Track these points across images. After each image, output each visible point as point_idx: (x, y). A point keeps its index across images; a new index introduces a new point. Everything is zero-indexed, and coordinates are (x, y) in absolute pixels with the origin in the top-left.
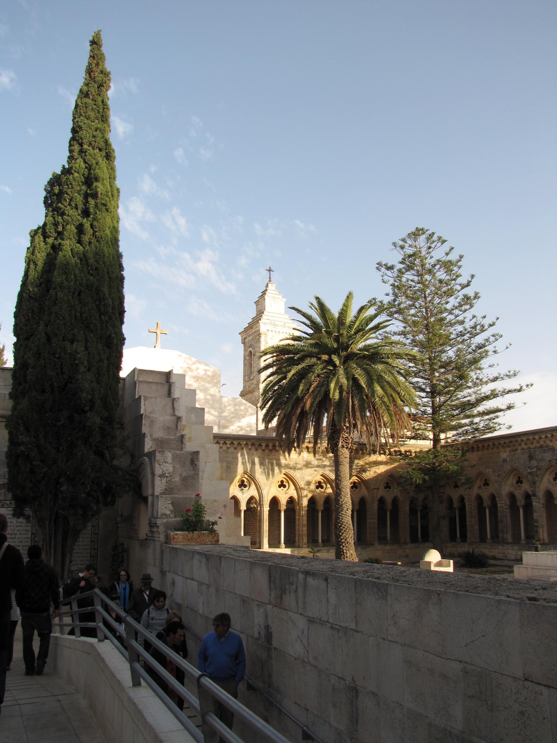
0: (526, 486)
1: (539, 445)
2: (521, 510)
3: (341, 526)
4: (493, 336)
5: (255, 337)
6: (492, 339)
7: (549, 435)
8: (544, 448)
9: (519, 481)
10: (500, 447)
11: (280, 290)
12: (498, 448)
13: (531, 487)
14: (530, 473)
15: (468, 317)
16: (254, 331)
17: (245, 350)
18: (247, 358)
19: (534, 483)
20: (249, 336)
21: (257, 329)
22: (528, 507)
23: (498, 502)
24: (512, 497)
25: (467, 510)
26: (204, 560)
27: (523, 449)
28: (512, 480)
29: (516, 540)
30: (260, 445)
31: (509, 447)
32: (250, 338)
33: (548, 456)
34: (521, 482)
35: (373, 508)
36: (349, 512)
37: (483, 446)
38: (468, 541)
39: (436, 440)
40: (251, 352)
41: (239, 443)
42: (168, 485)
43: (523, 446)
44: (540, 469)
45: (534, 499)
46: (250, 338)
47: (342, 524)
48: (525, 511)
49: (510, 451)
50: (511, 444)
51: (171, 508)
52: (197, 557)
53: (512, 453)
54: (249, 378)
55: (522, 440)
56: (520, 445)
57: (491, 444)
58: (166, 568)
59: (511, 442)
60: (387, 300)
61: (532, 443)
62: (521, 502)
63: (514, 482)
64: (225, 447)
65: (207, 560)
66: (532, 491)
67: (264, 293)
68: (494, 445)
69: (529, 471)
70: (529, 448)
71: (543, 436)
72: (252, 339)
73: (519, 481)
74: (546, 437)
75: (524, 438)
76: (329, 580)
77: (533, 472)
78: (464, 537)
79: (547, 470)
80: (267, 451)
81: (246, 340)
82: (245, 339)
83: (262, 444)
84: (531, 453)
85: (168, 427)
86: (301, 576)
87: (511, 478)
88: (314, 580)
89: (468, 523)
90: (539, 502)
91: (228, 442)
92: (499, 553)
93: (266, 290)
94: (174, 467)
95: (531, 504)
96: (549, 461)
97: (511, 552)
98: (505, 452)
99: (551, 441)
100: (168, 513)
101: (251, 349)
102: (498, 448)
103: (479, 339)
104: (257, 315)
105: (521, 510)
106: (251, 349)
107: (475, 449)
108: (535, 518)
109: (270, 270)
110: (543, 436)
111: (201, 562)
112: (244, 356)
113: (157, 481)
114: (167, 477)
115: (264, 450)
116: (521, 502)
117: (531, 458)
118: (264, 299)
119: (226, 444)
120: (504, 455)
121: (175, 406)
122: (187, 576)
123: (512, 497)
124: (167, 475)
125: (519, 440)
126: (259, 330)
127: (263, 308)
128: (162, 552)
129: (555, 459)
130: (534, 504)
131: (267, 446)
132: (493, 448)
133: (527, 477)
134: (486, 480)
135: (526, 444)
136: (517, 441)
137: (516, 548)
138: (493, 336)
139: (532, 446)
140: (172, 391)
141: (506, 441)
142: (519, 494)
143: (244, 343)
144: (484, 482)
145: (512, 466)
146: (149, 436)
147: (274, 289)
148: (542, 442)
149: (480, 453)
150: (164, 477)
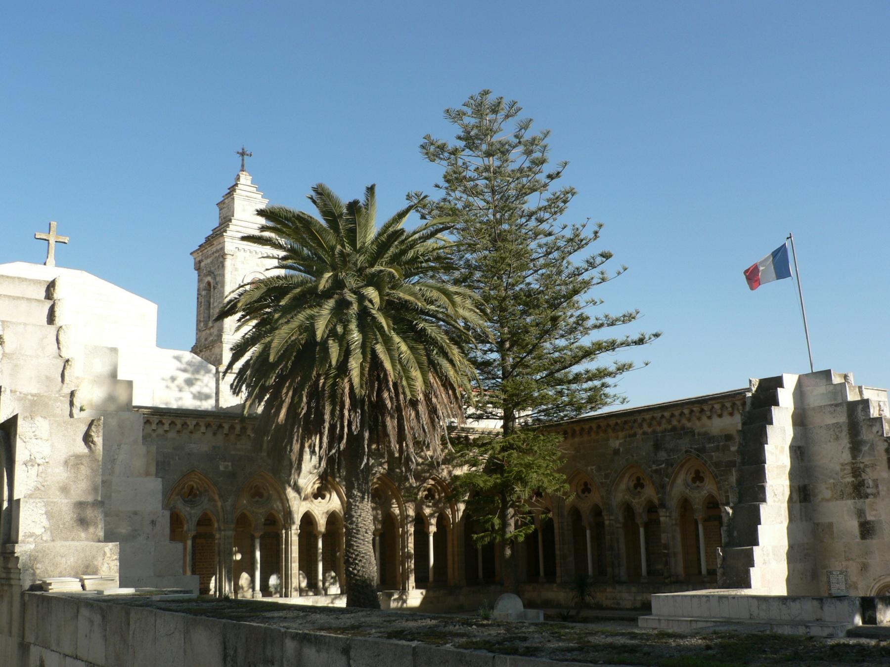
0: (650, 492)
1: (670, 427)
2: (642, 530)
3: (356, 559)
4: (602, 255)
5: (217, 258)
6: (599, 260)
7: (686, 411)
8: (679, 432)
9: (639, 484)
10: (610, 430)
11: (259, 184)
12: (605, 431)
13: (658, 493)
14: (656, 471)
15: (561, 225)
16: (214, 249)
17: (200, 281)
18: (204, 293)
19: (663, 486)
20: (207, 258)
21: (220, 246)
22: (652, 525)
23: (606, 518)
24: (628, 509)
25: (556, 531)
26: (97, 618)
27: (645, 433)
29: (634, 577)
30: (220, 427)
31: (623, 429)
32: (209, 261)
33: (684, 444)
34: (642, 486)
36: (370, 536)
37: (582, 430)
38: (558, 580)
39: (508, 418)
40: (209, 283)
41: (185, 423)
42: (40, 480)
43: (645, 428)
44: (672, 465)
45: (662, 512)
46: (209, 261)
47: (357, 555)
48: (646, 532)
49: (626, 437)
50: (627, 427)
51: (45, 522)
52: (85, 612)
53: (628, 439)
54: (206, 325)
55: (644, 420)
56: (641, 426)
57: (594, 426)
58: (30, 638)
59: (626, 422)
60: (436, 196)
61: (659, 424)
62: (641, 518)
63: (632, 484)
64: (160, 431)
65: (104, 617)
66: (659, 499)
67: (233, 189)
68: (599, 427)
69: (654, 467)
70: (654, 432)
71: (677, 413)
72: (212, 262)
73: (639, 484)
74: (682, 414)
75: (647, 416)
76: (352, 654)
77: (661, 469)
78: (551, 575)
79: (682, 466)
80: (232, 437)
81: (202, 264)
82: (200, 262)
83: (224, 425)
84: (657, 440)
85: (47, 378)
86: (290, 645)
87: (626, 480)
88: (318, 651)
89: (558, 552)
90: (670, 517)
91: (167, 421)
92: (606, 599)
93: (236, 185)
94: (52, 446)
95: (657, 522)
96: (686, 452)
97: (627, 597)
98: (617, 438)
99: (689, 420)
100: (39, 531)
101: (209, 279)
102: (605, 431)
103: (577, 260)
104: (220, 224)
105: (642, 530)
106: (209, 279)
107: (570, 434)
108: (663, 542)
109: (243, 154)
110: (677, 413)
111: (91, 622)
112: (198, 290)
113: (20, 471)
114: (39, 465)
115: (227, 435)
116: (641, 518)
117: (657, 446)
118: (233, 199)
119: (163, 424)
120: (615, 444)
121: (61, 338)
122: (67, 652)
123: (628, 509)
124: (39, 461)
125: (639, 419)
126: (223, 249)
127: (230, 214)
128: (24, 605)
129: (695, 449)
130: (662, 519)
131: (232, 428)
132: (597, 433)
133: (651, 477)
134: (586, 484)
135: (650, 426)
136: (635, 421)
137: (634, 589)
138: (602, 255)
139: (659, 429)
140: (57, 314)
141: (619, 421)
142: (638, 504)
143: (198, 268)
144: (583, 487)
145: (627, 460)
146: (8, 391)
147: (249, 183)
148: (675, 422)
149: (577, 440)
150: (33, 466)
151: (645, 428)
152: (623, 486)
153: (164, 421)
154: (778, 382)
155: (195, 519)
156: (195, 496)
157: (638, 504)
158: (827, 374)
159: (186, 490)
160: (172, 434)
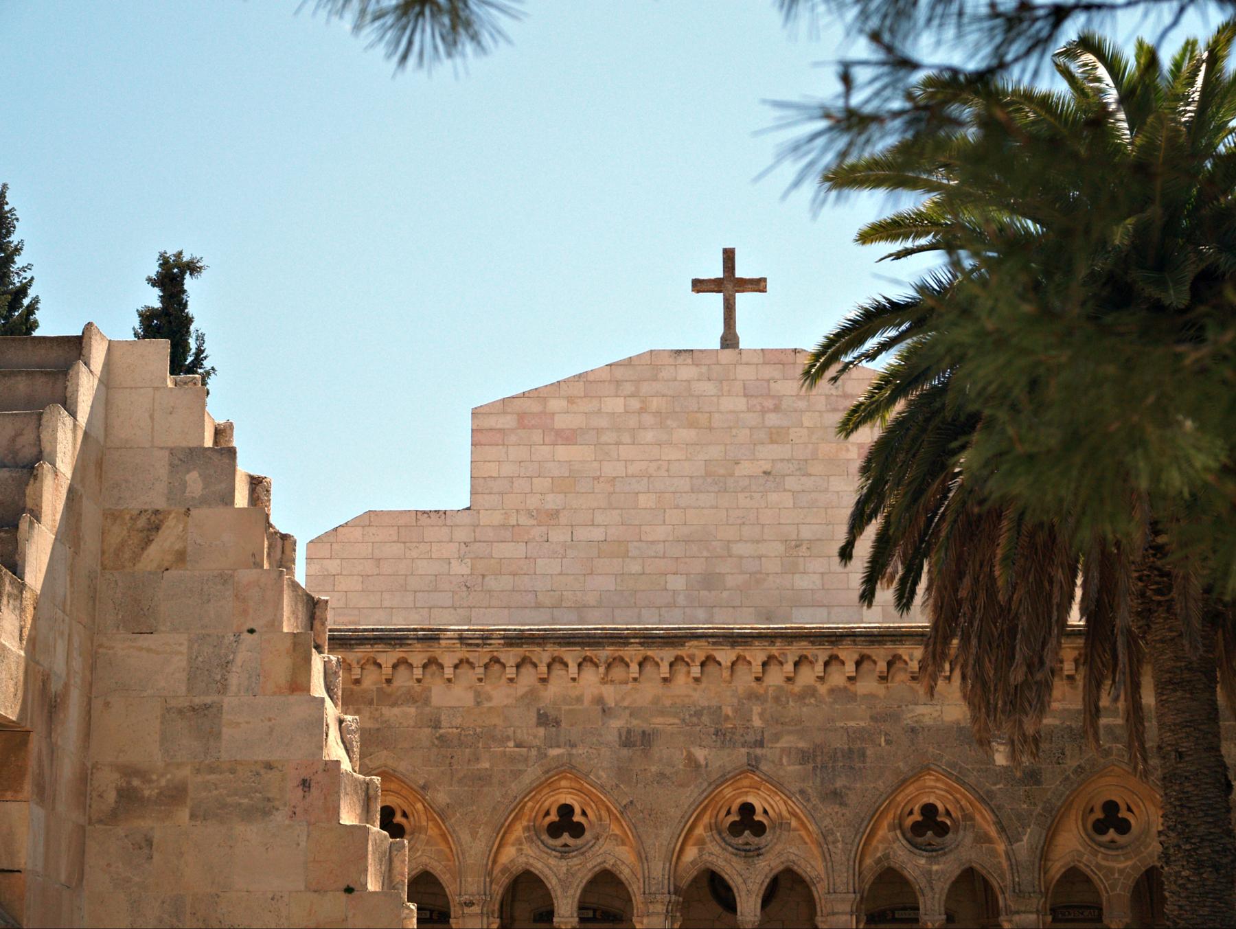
64: (837, 678)
91: (848, 654)
153: (842, 655)
155: (942, 886)
156: (942, 830)
159: (916, 817)
160: (868, 685)
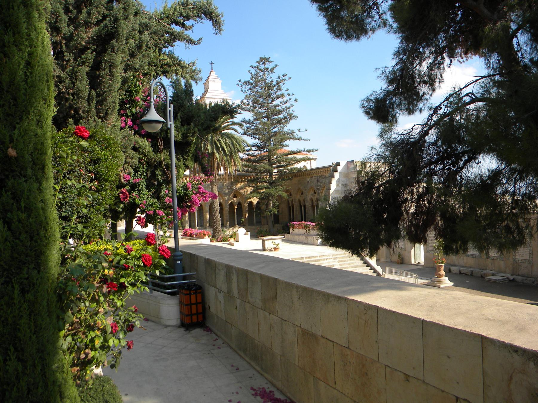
0: (316, 195)
9: (315, 193)
28: (312, 192)
35: (226, 209)
75: (315, 171)
117: (318, 181)
120: (308, 179)
142: (314, 199)
151: (315, 175)
152: (311, 193)
154: (338, 164)
157: (314, 199)
158: (353, 161)
